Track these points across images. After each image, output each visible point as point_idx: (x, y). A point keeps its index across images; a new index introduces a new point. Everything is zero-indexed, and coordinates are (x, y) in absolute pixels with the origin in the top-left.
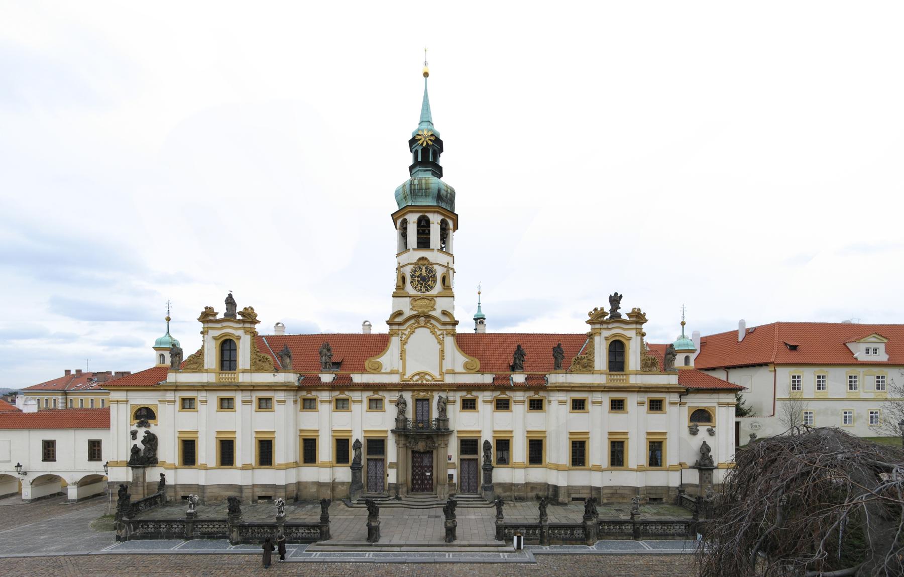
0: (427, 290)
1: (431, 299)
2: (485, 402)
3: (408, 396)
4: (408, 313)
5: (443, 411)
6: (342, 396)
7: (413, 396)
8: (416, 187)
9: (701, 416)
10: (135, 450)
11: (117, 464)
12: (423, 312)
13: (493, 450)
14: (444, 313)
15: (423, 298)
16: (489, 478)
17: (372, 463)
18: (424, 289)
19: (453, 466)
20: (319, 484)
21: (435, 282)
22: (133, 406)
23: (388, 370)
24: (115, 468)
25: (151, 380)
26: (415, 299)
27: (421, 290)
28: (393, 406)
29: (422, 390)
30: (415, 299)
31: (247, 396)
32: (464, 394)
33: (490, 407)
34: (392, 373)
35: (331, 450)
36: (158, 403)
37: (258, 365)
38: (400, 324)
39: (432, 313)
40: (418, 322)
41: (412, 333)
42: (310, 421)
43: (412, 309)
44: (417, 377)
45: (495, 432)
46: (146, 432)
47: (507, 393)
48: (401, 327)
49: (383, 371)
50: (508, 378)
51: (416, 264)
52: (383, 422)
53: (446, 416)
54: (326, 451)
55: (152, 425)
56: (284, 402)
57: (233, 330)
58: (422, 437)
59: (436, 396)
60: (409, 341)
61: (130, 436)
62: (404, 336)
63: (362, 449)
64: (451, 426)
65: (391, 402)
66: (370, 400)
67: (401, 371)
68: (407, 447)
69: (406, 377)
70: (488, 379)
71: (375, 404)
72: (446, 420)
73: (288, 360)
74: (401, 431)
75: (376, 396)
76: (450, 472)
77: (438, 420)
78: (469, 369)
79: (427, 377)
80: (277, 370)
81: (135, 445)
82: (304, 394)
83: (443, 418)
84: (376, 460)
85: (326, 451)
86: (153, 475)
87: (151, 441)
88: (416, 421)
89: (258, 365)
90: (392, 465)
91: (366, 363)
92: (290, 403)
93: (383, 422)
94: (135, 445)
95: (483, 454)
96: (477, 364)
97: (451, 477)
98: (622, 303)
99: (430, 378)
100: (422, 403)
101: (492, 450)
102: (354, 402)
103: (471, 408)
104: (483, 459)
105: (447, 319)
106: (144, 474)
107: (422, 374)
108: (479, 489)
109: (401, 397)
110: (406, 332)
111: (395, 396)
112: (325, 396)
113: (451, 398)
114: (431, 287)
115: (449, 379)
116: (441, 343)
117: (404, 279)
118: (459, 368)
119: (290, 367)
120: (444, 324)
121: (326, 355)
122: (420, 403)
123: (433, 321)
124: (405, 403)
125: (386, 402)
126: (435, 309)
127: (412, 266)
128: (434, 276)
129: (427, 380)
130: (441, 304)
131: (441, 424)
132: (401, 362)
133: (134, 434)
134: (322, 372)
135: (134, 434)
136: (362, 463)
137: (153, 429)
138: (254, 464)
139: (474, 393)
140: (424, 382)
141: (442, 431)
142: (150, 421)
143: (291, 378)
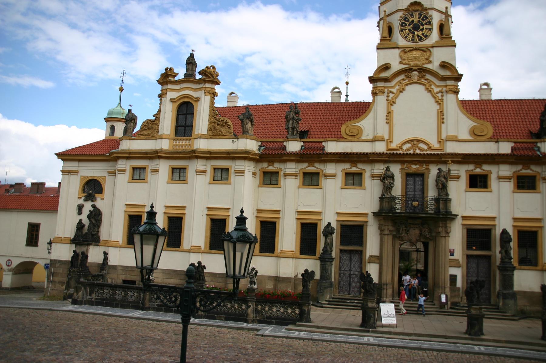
0: (420, 39)
1: (427, 49)
2: (500, 178)
3: (396, 169)
4: (396, 66)
5: (442, 187)
6: (311, 169)
7: (401, 169)
10: (80, 226)
12: (417, 65)
13: (513, 245)
14: (445, 65)
15: (416, 49)
16: (508, 282)
17: (345, 257)
18: (416, 39)
19: (456, 264)
20: (277, 279)
21: (430, 29)
23: (370, 137)
24: (58, 245)
25: (104, 153)
27: (413, 40)
28: (377, 182)
29: (415, 161)
30: (405, 50)
31: (200, 164)
32: (471, 167)
33: (508, 186)
35: (294, 236)
36: (105, 174)
37: (214, 132)
38: (386, 80)
39: (429, 66)
42: (271, 199)
43: (401, 63)
45: (515, 219)
46: (94, 206)
47: (533, 167)
48: (388, 84)
49: (364, 138)
50: (533, 147)
51: (407, 10)
52: (361, 202)
53: (447, 195)
54: (288, 237)
55: (98, 199)
56: (243, 172)
57: (190, 91)
58: (415, 220)
59: (434, 171)
60: (397, 101)
61: (76, 211)
62: (391, 95)
63: (334, 236)
64: (456, 208)
65: (373, 176)
66: (347, 175)
67: (386, 137)
68: (394, 237)
69: (393, 145)
70: (505, 148)
71: (353, 180)
72: (447, 201)
73: (249, 125)
74: (386, 214)
75: (354, 169)
76: (453, 271)
77: (437, 200)
78: (476, 135)
79: (421, 145)
80: (236, 137)
81: (81, 220)
82: (265, 165)
83: (443, 199)
84: (350, 252)
85: (288, 237)
86: (94, 255)
87: (96, 216)
88: (407, 199)
89: (214, 132)
90: (373, 260)
91: (343, 128)
92: (248, 175)
93: (361, 202)
94: (81, 220)
95: (498, 249)
96: (489, 130)
97: (453, 278)
99: (425, 147)
100: (415, 178)
101: (512, 244)
102: (326, 176)
103: (481, 187)
104: (498, 256)
105: (448, 73)
108: (493, 299)
109: (388, 169)
110: (394, 90)
111: (379, 169)
112: (292, 168)
113: (453, 173)
114: (426, 36)
115: (451, 148)
116: (439, 103)
117: (390, 30)
118: (465, 135)
119: (251, 132)
121: (293, 119)
122: (411, 180)
123: (428, 76)
124: (392, 177)
125: (367, 176)
126: (430, 62)
127: (401, 14)
128: (430, 23)
129: (420, 149)
130: (439, 56)
131: (441, 206)
132: (388, 125)
133: (80, 208)
134: (287, 140)
135: (80, 208)
136: (334, 255)
137: (99, 203)
138: (203, 247)
139: (486, 167)
140: (418, 151)
141: (444, 215)
142: (97, 195)
143: (251, 145)
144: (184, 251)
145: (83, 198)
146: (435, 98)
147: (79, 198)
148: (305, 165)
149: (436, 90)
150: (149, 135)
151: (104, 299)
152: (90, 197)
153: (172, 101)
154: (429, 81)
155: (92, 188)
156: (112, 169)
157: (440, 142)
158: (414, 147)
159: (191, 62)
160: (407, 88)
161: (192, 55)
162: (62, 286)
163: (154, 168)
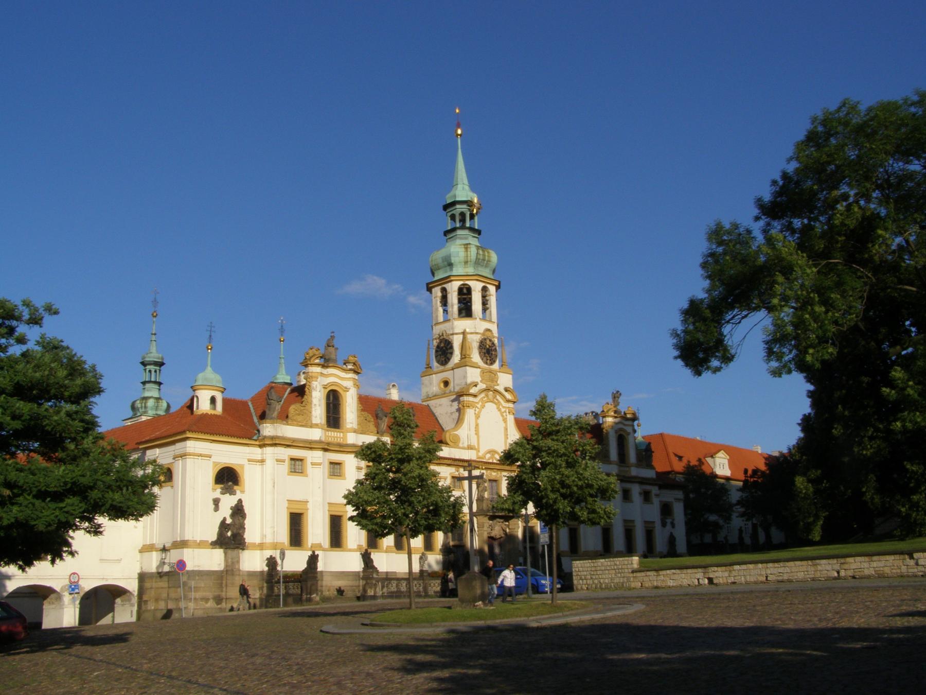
9: (666, 510)
11: (201, 545)
22: (215, 464)
26: (483, 372)
27: (486, 363)
34: (470, 448)
36: (245, 462)
40: (487, 396)
41: (483, 406)
44: (488, 456)
51: (483, 334)
55: (238, 492)
69: (480, 454)
98: (621, 400)
116: (505, 420)
120: (508, 401)
123: (498, 397)
133: (216, 502)
135: (216, 502)
142: (236, 487)
144: (350, 550)
145: (219, 490)
147: (214, 490)
149: (503, 410)
151: (392, 592)
152: (229, 491)
154: (499, 402)
155: (227, 477)
156: (259, 457)
158: (492, 457)
160: (487, 404)
161: (332, 337)
162: (207, 603)
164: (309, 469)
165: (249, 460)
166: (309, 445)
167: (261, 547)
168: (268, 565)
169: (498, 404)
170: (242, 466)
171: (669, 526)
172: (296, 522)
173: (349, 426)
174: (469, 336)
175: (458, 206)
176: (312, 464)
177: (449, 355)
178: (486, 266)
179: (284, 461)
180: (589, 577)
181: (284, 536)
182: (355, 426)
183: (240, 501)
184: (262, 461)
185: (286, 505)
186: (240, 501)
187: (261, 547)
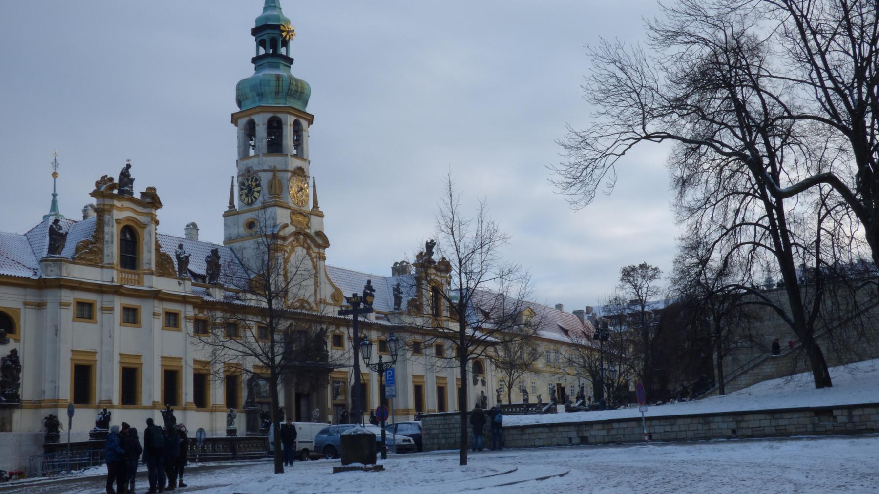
8: (294, 88)
38: (284, 239)
39: (308, 231)
41: (292, 250)
44: (298, 304)
55: (11, 341)
62: (286, 255)
106: (11, 417)
107: (303, 302)
109: (291, 325)
123: (309, 242)
126: (309, 228)
142: (9, 336)
144: (145, 408)
146: (313, 262)
148: (228, 315)
149: (314, 255)
150: (91, 260)
153: (118, 221)
157: (316, 304)
159: (125, 175)
161: (129, 166)
163: (106, 305)
164: (98, 314)
165: (25, 304)
166: (100, 289)
167: (37, 405)
168: (46, 425)
169: (308, 249)
170: (17, 311)
171: (479, 383)
172: (83, 376)
173: (146, 267)
174: (279, 174)
175: (269, 31)
176: (102, 309)
177: (256, 194)
178: (299, 99)
179: (68, 305)
180: (441, 436)
181: (66, 391)
182: (154, 268)
183: (14, 352)
184: (40, 306)
185: (70, 355)
186: (14, 352)
187: (37, 405)
